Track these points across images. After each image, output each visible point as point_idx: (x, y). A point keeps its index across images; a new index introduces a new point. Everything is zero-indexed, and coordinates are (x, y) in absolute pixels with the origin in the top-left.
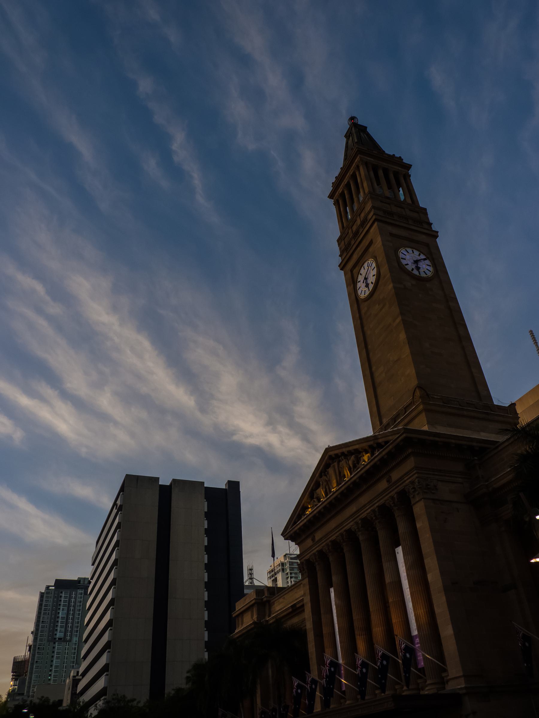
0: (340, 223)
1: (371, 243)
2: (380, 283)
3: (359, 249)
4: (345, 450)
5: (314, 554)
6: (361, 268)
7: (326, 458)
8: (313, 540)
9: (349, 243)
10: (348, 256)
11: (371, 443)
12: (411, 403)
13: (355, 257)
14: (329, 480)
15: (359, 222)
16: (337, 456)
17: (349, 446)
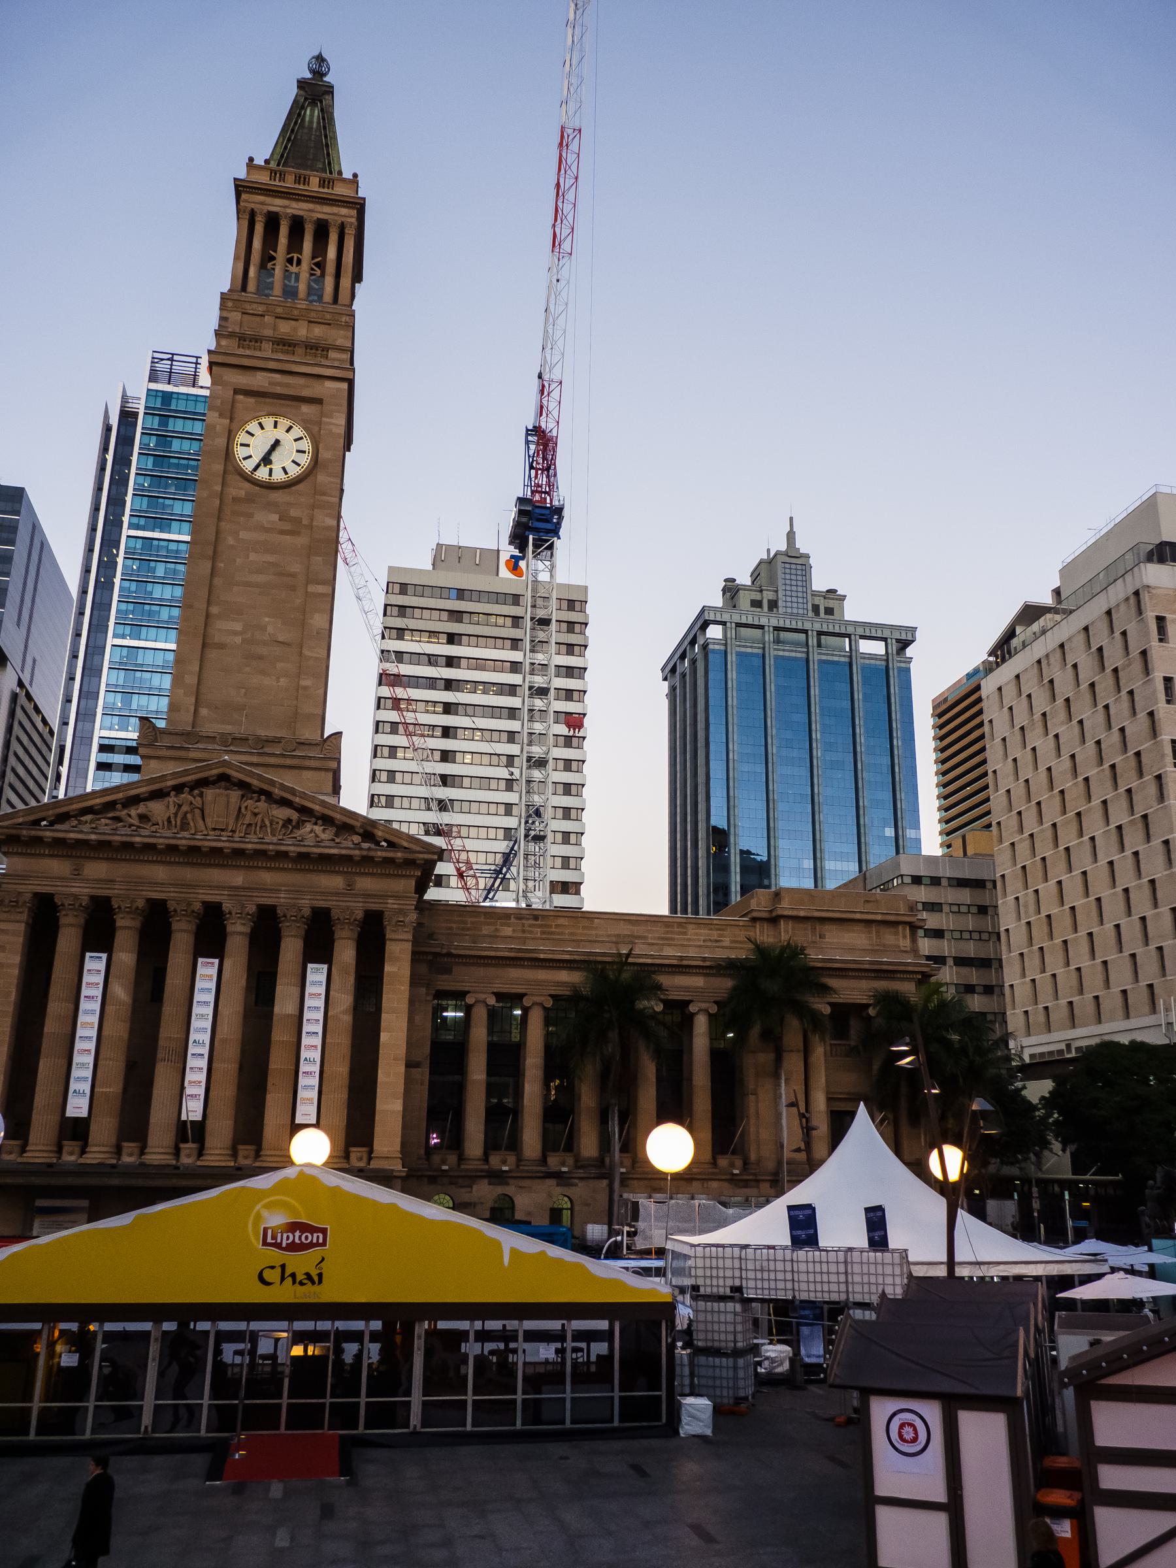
0: (241, 265)
1: (318, 401)
2: (300, 487)
3: (277, 376)
4: (276, 791)
5: (76, 897)
6: (269, 415)
7: (215, 772)
8: (77, 872)
9: (257, 340)
10: (246, 362)
11: (358, 824)
12: (317, 745)
13: (259, 381)
14: (202, 811)
15: (302, 331)
16: (242, 785)
17: (294, 795)
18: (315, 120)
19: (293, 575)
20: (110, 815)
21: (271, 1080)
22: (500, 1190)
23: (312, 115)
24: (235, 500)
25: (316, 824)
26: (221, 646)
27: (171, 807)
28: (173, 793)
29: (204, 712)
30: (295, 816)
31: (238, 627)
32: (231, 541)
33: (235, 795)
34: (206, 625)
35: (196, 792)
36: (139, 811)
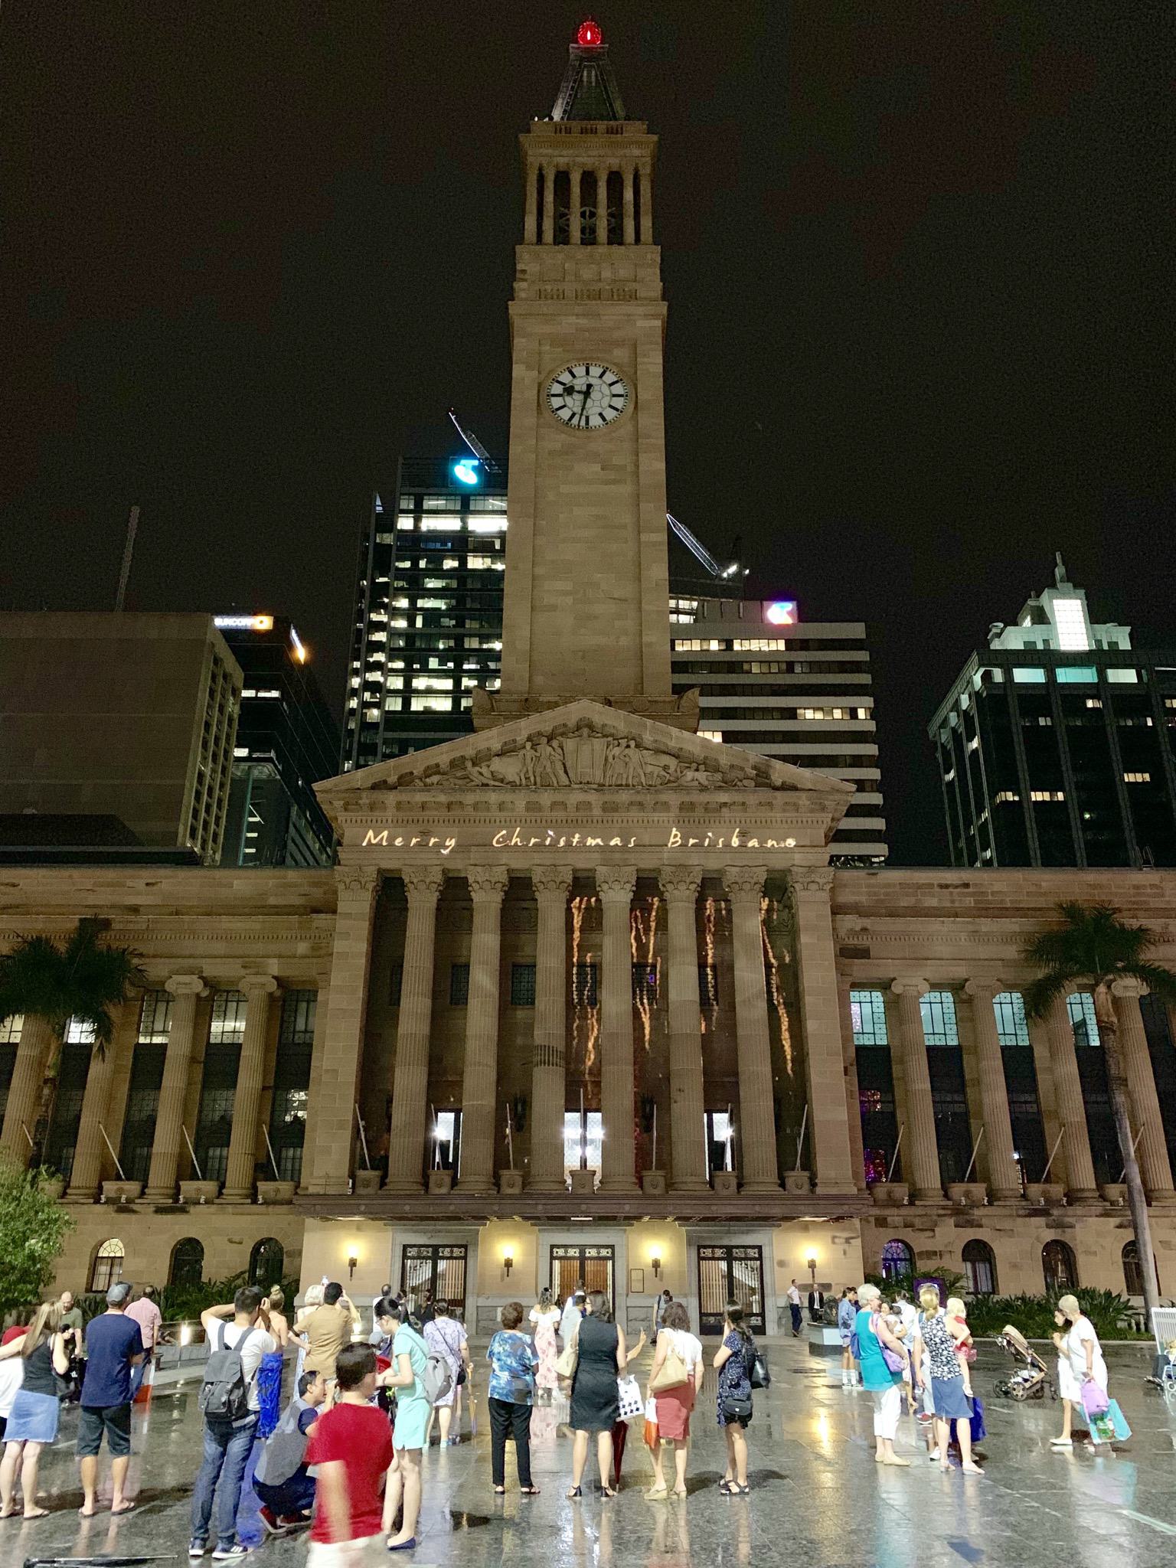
18: (593, 79)
19: (625, 527)
20: (459, 774)
21: (675, 1084)
22: (971, 1234)
23: (589, 76)
24: (552, 453)
25: (697, 770)
26: (553, 608)
27: (528, 760)
28: (529, 745)
29: (539, 680)
30: (672, 763)
31: (568, 586)
32: (551, 496)
33: (598, 744)
34: (533, 587)
35: (555, 743)
36: (492, 768)
